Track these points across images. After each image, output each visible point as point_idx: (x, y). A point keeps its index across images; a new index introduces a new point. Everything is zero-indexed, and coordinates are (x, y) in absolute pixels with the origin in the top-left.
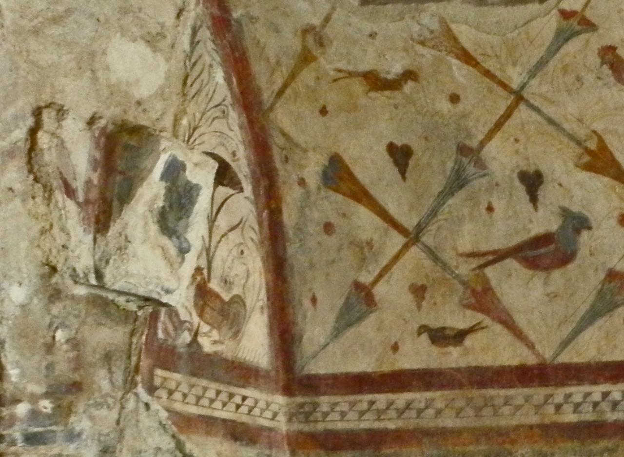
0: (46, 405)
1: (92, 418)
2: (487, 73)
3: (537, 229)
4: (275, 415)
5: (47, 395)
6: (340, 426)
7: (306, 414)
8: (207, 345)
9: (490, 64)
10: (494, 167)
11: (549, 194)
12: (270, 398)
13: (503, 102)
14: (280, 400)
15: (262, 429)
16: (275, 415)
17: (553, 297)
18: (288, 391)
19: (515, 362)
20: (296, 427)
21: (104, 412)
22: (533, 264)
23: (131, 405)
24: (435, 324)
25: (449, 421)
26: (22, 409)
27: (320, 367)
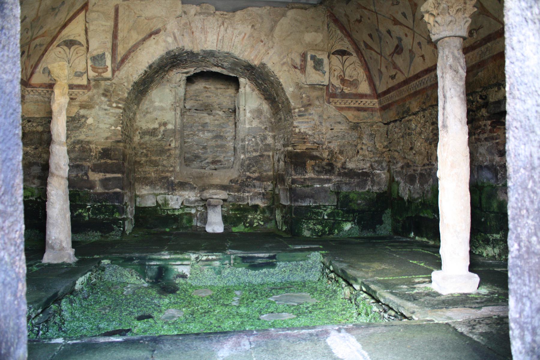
0: (303, 109)
1: (315, 110)
2: (369, 10)
3: (395, 44)
4: (374, 104)
5: (302, 107)
6: (384, 104)
7: (380, 103)
8: (346, 91)
9: (368, 8)
10: (382, 32)
11: (393, 34)
12: (372, 100)
13: (375, 16)
14: (376, 100)
15: (368, 108)
16: (374, 104)
17: (403, 60)
18: (377, 98)
19: (402, 80)
20: (381, 106)
21: (318, 109)
22: (399, 53)
23: (325, 106)
24: (391, 75)
25: (397, 98)
26: (297, 110)
27: (380, 91)
